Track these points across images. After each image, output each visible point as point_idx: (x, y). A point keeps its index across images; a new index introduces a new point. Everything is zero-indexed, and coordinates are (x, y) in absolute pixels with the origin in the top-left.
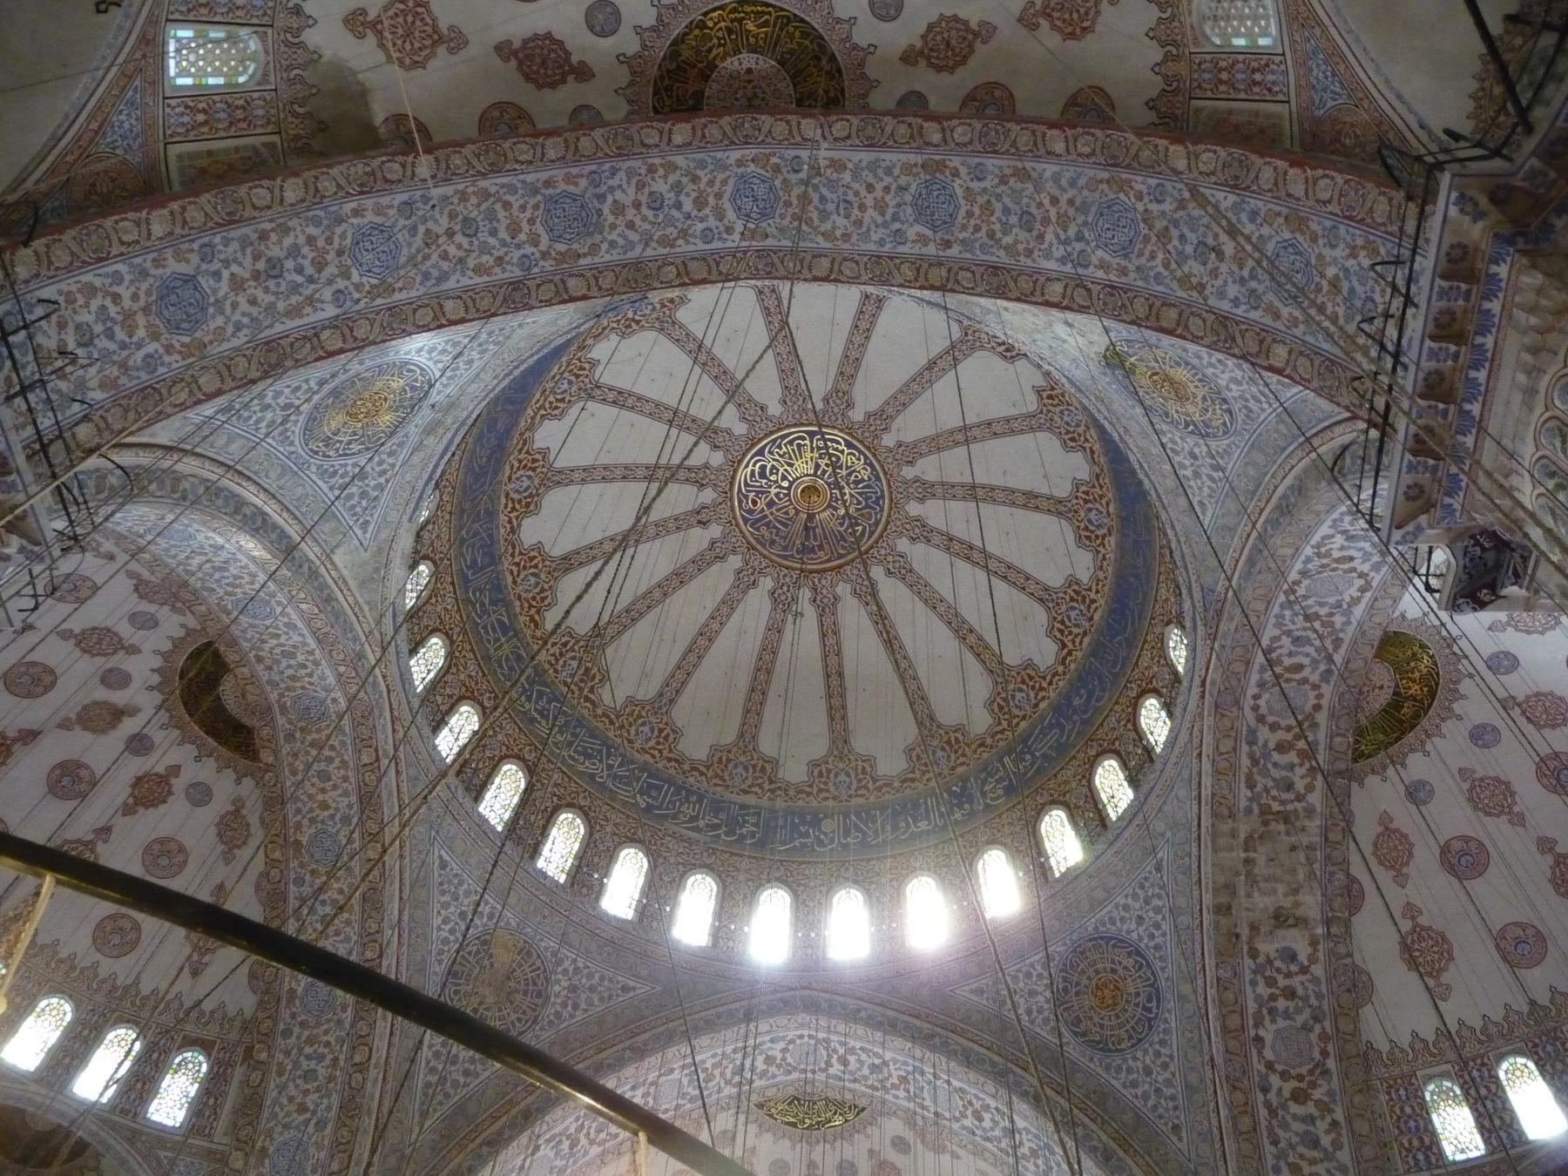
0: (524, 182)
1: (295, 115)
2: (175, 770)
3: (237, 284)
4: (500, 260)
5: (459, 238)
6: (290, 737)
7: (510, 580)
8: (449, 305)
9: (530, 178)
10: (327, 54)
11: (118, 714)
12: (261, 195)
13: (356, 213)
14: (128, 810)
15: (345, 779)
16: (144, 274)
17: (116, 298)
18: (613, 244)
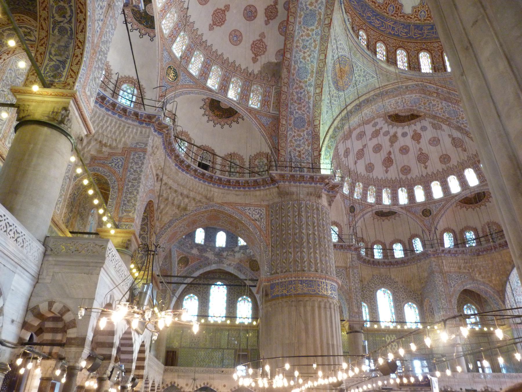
0: (298, 30)
1: (270, 81)
2: (415, 131)
3: (300, 109)
4: (315, 41)
5: (306, 51)
6: (420, 108)
7: (418, 22)
8: (321, 58)
9: (297, 28)
10: (260, 69)
11: (395, 136)
12: (283, 97)
13: (293, 75)
14: (419, 143)
15: (438, 101)
16: (292, 128)
17: (294, 136)
18: (320, 8)
